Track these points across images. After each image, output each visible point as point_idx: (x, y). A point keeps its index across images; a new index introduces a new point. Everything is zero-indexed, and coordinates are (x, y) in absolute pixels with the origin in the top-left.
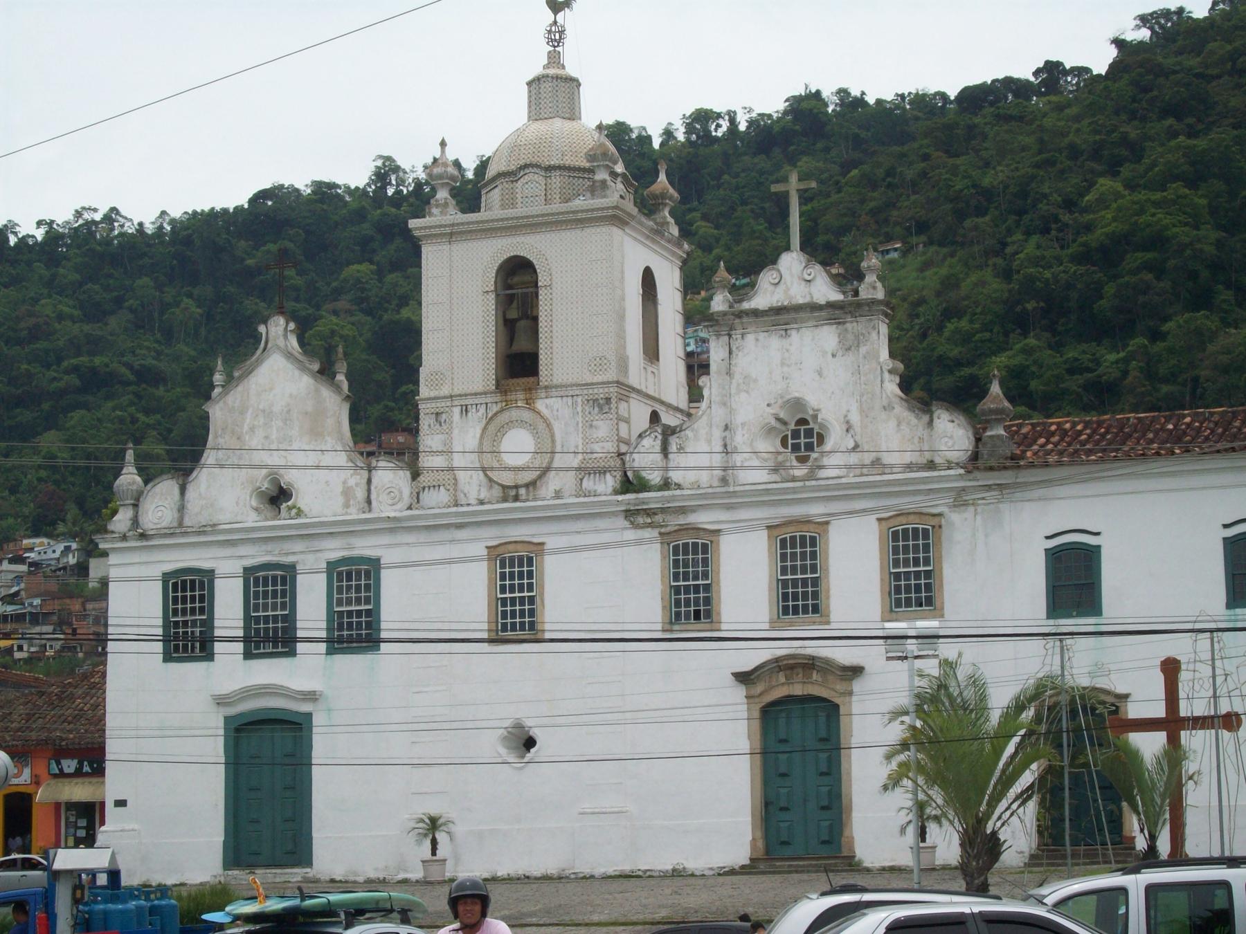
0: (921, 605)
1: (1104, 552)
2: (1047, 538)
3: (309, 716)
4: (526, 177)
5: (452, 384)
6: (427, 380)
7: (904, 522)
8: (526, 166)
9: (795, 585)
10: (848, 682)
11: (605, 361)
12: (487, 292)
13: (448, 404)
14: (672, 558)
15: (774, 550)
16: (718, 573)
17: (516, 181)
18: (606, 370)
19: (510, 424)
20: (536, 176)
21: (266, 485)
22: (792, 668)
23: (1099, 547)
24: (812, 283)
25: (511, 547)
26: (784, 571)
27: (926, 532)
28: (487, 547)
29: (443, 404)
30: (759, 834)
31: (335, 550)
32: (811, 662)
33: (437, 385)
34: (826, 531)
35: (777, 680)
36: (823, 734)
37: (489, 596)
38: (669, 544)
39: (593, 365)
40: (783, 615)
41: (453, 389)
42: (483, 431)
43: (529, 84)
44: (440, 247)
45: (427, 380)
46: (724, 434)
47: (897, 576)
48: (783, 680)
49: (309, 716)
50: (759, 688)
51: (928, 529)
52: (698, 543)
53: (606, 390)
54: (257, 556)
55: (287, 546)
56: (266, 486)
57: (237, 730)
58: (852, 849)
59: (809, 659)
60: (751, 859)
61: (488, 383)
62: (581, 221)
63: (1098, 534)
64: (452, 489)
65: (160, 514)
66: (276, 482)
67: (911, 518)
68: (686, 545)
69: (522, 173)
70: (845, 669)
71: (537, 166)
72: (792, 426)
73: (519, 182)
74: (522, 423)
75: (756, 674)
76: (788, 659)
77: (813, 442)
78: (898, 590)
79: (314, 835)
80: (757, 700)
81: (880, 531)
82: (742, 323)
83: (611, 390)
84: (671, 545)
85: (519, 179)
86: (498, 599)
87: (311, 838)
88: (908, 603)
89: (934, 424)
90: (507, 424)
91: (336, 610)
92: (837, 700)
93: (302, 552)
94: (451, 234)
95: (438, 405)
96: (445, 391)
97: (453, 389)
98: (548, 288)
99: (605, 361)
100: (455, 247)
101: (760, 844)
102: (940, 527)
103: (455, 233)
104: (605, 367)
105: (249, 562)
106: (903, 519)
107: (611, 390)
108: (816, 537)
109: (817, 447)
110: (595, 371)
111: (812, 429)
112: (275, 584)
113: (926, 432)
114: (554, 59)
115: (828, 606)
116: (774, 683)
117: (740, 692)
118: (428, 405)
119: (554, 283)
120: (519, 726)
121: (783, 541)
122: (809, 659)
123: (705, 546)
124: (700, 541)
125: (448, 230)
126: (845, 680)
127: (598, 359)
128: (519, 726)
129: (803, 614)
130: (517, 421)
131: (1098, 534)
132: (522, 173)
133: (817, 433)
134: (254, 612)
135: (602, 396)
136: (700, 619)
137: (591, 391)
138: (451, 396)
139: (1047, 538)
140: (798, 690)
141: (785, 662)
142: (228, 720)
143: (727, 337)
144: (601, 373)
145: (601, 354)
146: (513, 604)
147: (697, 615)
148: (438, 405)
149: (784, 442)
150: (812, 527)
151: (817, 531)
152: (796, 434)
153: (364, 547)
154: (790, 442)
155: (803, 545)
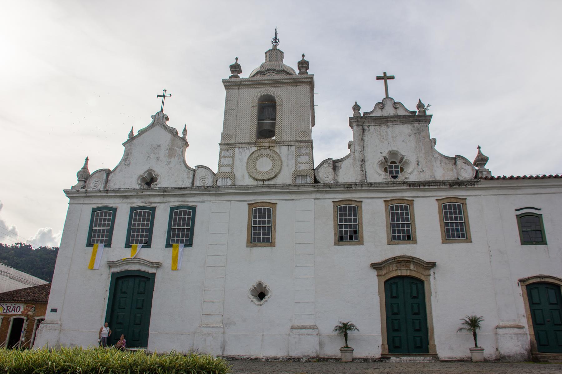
0: (459, 237)
1: (543, 216)
2: (516, 210)
3: (154, 274)
4: (269, 74)
5: (236, 140)
6: (224, 137)
7: (449, 201)
8: (270, 70)
9: (398, 227)
10: (428, 270)
11: (306, 133)
12: (254, 106)
13: (233, 146)
14: (338, 212)
15: (388, 210)
16: (362, 219)
17: (265, 75)
18: (306, 136)
19: (261, 156)
20: (273, 73)
21: (146, 175)
22: (399, 262)
23: (541, 215)
24: (397, 109)
25: (260, 204)
26: (393, 220)
27: (459, 206)
28: (248, 204)
29: (231, 147)
30: (386, 342)
31: (175, 202)
32: (411, 260)
33: (228, 139)
34: (413, 204)
35: (393, 269)
36: (415, 294)
37: (248, 225)
38: (337, 206)
39: (300, 135)
40: (393, 240)
41: (236, 141)
42: (249, 157)
43: (265, 53)
44: (234, 90)
45: (224, 137)
46: (361, 163)
47: (447, 224)
48: (395, 268)
49: (154, 274)
50: (384, 272)
51: (460, 205)
52: (351, 206)
53: (307, 144)
54: (138, 202)
55: (152, 200)
56: (146, 175)
57: (118, 279)
58: (435, 351)
59: (410, 259)
60: (382, 355)
61: (252, 139)
62: (296, 83)
63: (540, 209)
64: (233, 180)
65: (96, 184)
66: (150, 174)
67: (452, 200)
68: (345, 207)
69: (267, 72)
70: (429, 263)
71: (274, 70)
72: (389, 164)
73: (266, 75)
74: (267, 156)
75: (383, 265)
76: (399, 258)
77: (399, 171)
78: (448, 230)
79: (150, 332)
80: (383, 277)
81: (438, 205)
82: (369, 121)
83: (309, 144)
84: (338, 207)
85: (266, 74)
86: (252, 226)
87: (148, 334)
88: (453, 237)
89: (457, 164)
90: (260, 155)
91: (172, 228)
92: (423, 278)
93: (159, 203)
94: (240, 85)
95: (229, 147)
96: (233, 141)
97: (236, 141)
98: (281, 106)
99: (306, 133)
100: (240, 91)
101: (387, 346)
102: (466, 204)
103: (241, 85)
104: (306, 135)
105: (134, 206)
106: (448, 200)
107: (309, 144)
108: (408, 206)
109: (401, 172)
110: (302, 137)
111: (398, 165)
112: (144, 215)
113: (454, 166)
114: (275, 46)
115: (415, 236)
116: (391, 269)
117: (374, 273)
118: (224, 147)
119: (283, 104)
120: (260, 285)
121: (392, 208)
122: (410, 259)
123: (354, 208)
124: (352, 206)
125: (239, 83)
126: (427, 269)
127: (303, 132)
128: (260, 285)
129: (403, 239)
130: (265, 154)
131: (540, 209)
132: (267, 72)
133: (400, 167)
134: (133, 227)
135: (305, 146)
136: (353, 240)
137: (299, 144)
138: (235, 143)
139: (516, 210)
140: (404, 273)
141: (398, 259)
142: (113, 274)
143: (361, 127)
144: (304, 137)
145: (304, 130)
146: (259, 229)
147: (351, 238)
148: (229, 147)
149: (386, 170)
150: (405, 202)
151: (409, 204)
152: (391, 167)
153: (191, 201)
154: (388, 170)
155: (402, 209)
